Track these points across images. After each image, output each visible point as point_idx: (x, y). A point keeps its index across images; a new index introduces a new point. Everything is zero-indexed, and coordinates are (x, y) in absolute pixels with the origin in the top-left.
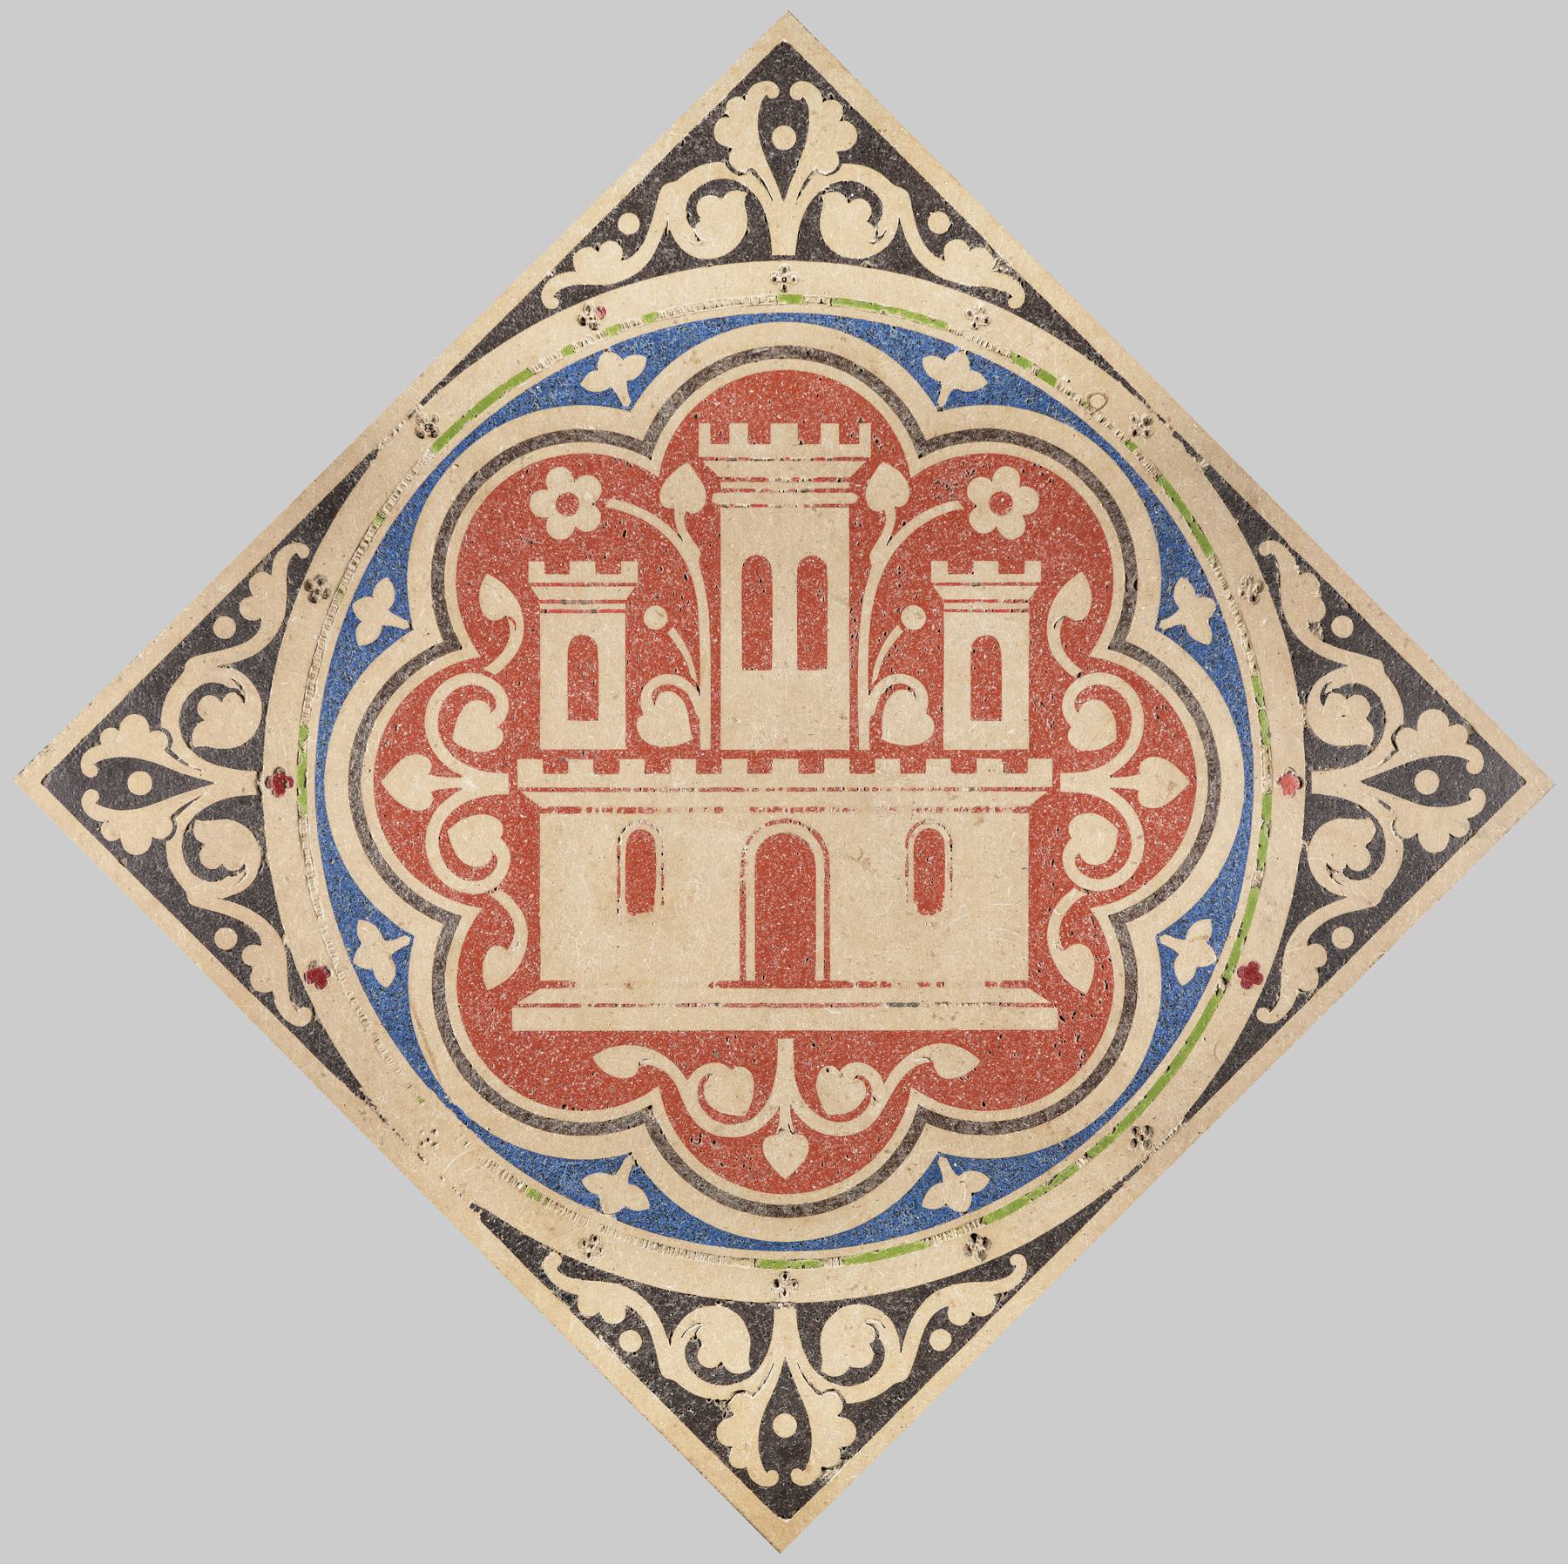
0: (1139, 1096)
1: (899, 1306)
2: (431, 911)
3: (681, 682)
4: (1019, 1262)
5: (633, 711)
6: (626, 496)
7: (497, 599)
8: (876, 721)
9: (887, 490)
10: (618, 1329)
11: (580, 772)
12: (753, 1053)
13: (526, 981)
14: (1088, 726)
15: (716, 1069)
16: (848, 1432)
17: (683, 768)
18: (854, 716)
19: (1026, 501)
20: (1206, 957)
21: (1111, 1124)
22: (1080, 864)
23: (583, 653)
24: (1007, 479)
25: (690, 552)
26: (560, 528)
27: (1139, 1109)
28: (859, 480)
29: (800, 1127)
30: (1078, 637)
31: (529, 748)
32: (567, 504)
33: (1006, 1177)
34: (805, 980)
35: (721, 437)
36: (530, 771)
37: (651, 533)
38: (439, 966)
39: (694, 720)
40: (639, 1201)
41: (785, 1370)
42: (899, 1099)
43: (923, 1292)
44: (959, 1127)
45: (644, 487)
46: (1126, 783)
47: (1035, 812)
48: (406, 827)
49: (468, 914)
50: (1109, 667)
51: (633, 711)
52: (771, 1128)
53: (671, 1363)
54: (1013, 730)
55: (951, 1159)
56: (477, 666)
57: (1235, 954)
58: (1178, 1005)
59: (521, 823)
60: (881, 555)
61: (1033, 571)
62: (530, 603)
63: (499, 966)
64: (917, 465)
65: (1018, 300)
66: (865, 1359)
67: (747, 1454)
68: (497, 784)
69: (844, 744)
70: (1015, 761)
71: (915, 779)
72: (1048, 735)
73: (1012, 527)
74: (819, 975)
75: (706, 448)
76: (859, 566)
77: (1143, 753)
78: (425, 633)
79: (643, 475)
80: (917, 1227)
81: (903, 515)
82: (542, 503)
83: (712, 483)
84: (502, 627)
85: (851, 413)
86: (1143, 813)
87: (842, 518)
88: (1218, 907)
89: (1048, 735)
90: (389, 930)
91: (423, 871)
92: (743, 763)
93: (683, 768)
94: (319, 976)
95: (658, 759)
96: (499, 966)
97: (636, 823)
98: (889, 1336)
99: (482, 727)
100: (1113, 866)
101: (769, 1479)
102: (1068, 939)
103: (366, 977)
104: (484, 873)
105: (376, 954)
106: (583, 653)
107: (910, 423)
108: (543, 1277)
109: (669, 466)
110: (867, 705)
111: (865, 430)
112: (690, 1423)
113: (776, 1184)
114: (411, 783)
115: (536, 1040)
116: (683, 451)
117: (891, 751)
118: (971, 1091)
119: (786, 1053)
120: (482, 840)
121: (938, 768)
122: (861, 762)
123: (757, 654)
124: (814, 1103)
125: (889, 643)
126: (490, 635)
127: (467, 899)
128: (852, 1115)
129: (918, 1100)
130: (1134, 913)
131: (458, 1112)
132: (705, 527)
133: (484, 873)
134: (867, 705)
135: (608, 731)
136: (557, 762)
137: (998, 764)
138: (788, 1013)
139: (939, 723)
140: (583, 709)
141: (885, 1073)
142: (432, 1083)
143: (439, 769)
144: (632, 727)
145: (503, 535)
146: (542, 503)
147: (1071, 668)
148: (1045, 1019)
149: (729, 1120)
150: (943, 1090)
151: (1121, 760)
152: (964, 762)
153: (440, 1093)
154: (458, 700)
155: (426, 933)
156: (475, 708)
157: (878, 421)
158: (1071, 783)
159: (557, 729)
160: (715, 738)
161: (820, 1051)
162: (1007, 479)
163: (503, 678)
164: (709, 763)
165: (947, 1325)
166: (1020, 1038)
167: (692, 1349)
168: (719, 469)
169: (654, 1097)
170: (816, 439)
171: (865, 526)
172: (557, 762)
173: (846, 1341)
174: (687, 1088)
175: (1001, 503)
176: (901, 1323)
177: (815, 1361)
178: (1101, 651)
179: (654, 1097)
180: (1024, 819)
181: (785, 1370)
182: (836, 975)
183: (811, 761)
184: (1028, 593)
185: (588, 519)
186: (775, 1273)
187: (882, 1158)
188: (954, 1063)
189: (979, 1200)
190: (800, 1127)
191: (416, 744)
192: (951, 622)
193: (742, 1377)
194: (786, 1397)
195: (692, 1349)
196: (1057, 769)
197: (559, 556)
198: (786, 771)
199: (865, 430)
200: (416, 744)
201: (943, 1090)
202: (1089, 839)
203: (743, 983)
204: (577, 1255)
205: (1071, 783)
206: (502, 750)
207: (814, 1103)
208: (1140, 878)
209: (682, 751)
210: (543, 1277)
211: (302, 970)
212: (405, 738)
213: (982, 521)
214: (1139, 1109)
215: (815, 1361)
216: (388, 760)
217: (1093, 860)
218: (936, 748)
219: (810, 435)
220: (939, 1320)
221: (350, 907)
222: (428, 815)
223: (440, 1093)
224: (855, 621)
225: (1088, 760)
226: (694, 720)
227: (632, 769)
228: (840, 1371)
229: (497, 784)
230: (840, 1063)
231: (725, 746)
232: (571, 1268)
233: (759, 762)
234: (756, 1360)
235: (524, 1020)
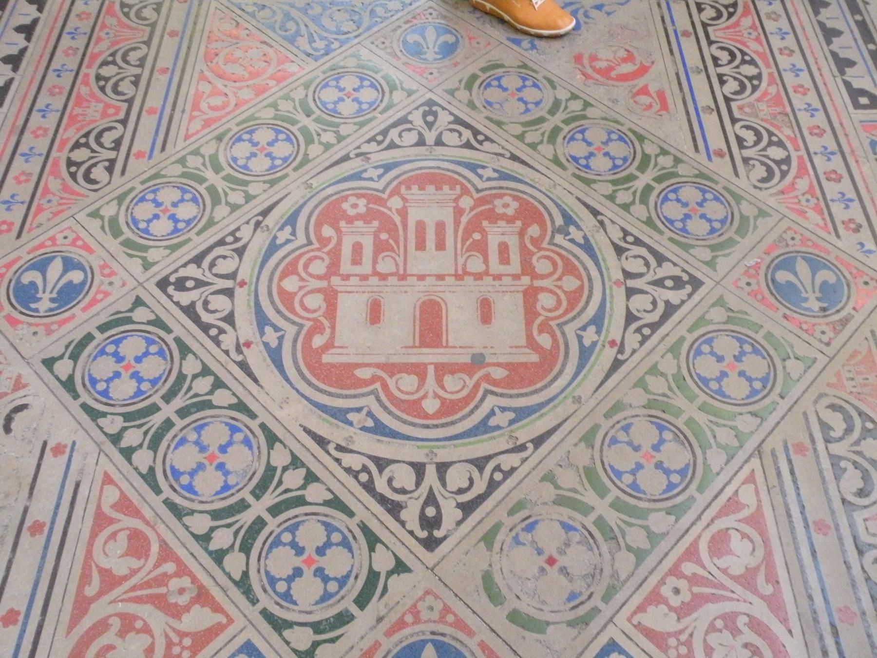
0: (574, 385)
1: (479, 463)
2: (294, 323)
3: (393, 255)
4: (530, 446)
5: (375, 262)
6: (375, 203)
7: (327, 231)
8: (465, 265)
9: (466, 202)
10: (358, 472)
11: (354, 280)
12: (419, 370)
13: (329, 345)
14: (542, 266)
15: (404, 375)
16: (459, 514)
17: (393, 280)
18: (456, 265)
19: (515, 205)
20: (595, 338)
21: (563, 395)
22: (543, 308)
23: (357, 249)
24: (507, 199)
25: (397, 219)
26: (351, 212)
27: (574, 389)
28: (456, 200)
29: (436, 396)
30: (536, 242)
31: (336, 273)
32: (355, 206)
33: (522, 414)
34: (438, 345)
35: (409, 188)
36: (336, 281)
37: (383, 213)
38: (295, 341)
39: (397, 265)
40: (370, 423)
41: (431, 489)
42: (477, 386)
43: (489, 458)
44: (502, 395)
45: (382, 202)
46: (559, 283)
47: (525, 293)
48: (287, 297)
49: (308, 324)
50: (548, 250)
51: (375, 262)
52: (425, 397)
53: (381, 486)
54: (515, 266)
55: (499, 407)
56: (318, 250)
57: (606, 337)
58: (585, 353)
59: (331, 297)
60: (464, 220)
61: (519, 223)
62: (338, 230)
63: (318, 341)
64: (476, 195)
65: (508, 155)
66: (466, 484)
67: (414, 524)
68: (323, 284)
69: (453, 272)
70: (516, 277)
71: (480, 283)
72: (527, 268)
73: (510, 212)
74: (444, 344)
75: (403, 190)
76: (457, 223)
77: (563, 274)
78: (301, 239)
79: (381, 199)
80: (486, 432)
81: (472, 209)
82: (345, 206)
83: (404, 199)
84: (329, 239)
85: (453, 183)
86: (565, 292)
87: (451, 210)
88: (598, 321)
89: (527, 268)
90: (277, 329)
91: (292, 310)
92: (415, 278)
93: (393, 280)
94: (248, 344)
95: (383, 277)
96: (318, 341)
97: (375, 296)
98: (476, 475)
99: (319, 268)
100: (556, 309)
101: (424, 534)
102: (541, 332)
103: (266, 345)
104: (315, 311)
105: (271, 337)
106: (357, 249)
107: (474, 185)
108: (328, 452)
109: (391, 195)
110: (461, 261)
111: (458, 187)
112: (389, 511)
113: (426, 416)
114: (290, 284)
115: (332, 366)
116: (395, 192)
117: (469, 274)
118: (506, 383)
119: (431, 370)
120: (315, 301)
121: (488, 280)
122: (458, 277)
123: (421, 245)
124: (443, 387)
125: (468, 243)
126: (324, 241)
127: (308, 319)
128: (457, 392)
129: (484, 386)
130: (566, 323)
131: (298, 391)
132: (403, 213)
133: (315, 311)
134: (461, 261)
135: (366, 268)
136: (346, 277)
137: (510, 278)
138: (430, 356)
139: (487, 266)
140: (357, 260)
141: (471, 377)
142: (287, 380)
143: (302, 279)
144: (374, 267)
145: (332, 214)
146: (345, 206)
147: (535, 250)
148: (534, 358)
149: (407, 393)
150: (495, 383)
151: (556, 276)
152: (498, 277)
153: (291, 384)
154: (311, 260)
155: (290, 330)
156: (317, 261)
157: (462, 185)
158: (538, 283)
159: (346, 267)
160: (405, 270)
161: (443, 370)
162: (507, 199)
163: (328, 253)
164: (403, 277)
165: (501, 471)
166: (524, 365)
167: (390, 481)
168: (408, 197)
169: (377, 385)
170: (441, 189)
171: (458, 212)
172: (346, 277)
173: (457, 477)
174: (391, 383)
175: (506, 206)
176: (481, 470)
177: (444, 484)
178: (545, 245)
179: (377, 385)
180: (520, 295)
181: (431, 489)
182: (450, 344)
183: (441, 277)
184: (518, 229)
185: (362, 209)
186: (426, 451)
187: (472, 406)
188: (499, 373)
189: (512, 422)
190: (436, 396)
191: (295, 272)
192: (490, 237)
193: (411, 492)
194: (431, 499)
195: (390, 481)
196: (532, 279)
197: (350, 220)
198: (429, 280)
199: (458, 187)
200: (295, 272)
201: (495, 383)
202: (545, 301)
203: (414, 347)
204: (343, 444)
205: (538, 283)
206: (325, 275)
207: (443, 387)
208: (567, 312)
209: (392, 274)
210: (328, 452)
211: (242, 341)
212: (291, 270)
213: (500, 210)
214: (574, 389)
215: (444, 484)
216: (282, 277)
217: (548, 306)
218: (487, 273)
219: (439, 188)
220: (498, 468)
221: (262, 321)
222: (295, 294)
223: (291, 384)
224: (456, 237)
225: (543, 277)
226: (397, 265)
227: (374, 280)
228: (455, 489)
229: (323, 284)
230: (453, 373)
231: (409, 272)
232: (339, 448)
233: (421, 278)
234: (418, 484)
235: (326, 358)
